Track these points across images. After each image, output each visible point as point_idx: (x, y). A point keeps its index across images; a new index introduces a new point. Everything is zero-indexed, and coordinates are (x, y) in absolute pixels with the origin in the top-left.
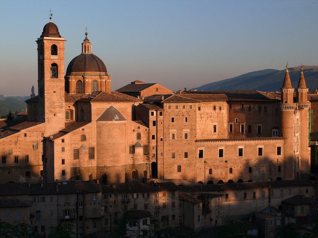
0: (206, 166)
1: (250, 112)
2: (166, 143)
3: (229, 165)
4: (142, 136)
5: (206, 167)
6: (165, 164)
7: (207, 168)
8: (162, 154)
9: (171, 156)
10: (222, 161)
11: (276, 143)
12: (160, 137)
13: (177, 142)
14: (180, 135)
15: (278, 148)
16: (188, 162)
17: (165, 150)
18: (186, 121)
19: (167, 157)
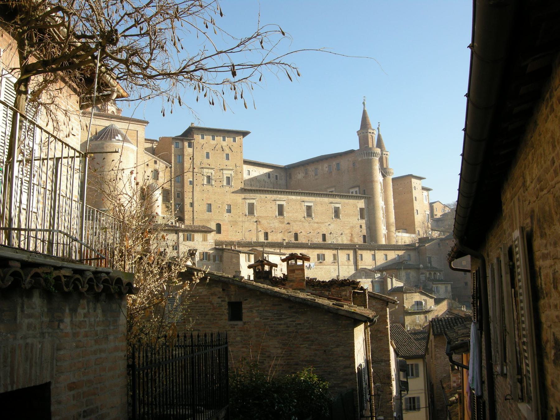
0: (259, 226)
1: (316, 177)
2: (197, 189)
3: (295, 228)
4: (161, 175)
5: (259, 229)
6: (195, 219)
8: (192, 205)
9: (205, 208)
10: (282, 223)
12: (189, 178)
13: (216, 189)
15: (360, 209)
17: (195, 199)
18: (228, 158)
19: (200, 207)
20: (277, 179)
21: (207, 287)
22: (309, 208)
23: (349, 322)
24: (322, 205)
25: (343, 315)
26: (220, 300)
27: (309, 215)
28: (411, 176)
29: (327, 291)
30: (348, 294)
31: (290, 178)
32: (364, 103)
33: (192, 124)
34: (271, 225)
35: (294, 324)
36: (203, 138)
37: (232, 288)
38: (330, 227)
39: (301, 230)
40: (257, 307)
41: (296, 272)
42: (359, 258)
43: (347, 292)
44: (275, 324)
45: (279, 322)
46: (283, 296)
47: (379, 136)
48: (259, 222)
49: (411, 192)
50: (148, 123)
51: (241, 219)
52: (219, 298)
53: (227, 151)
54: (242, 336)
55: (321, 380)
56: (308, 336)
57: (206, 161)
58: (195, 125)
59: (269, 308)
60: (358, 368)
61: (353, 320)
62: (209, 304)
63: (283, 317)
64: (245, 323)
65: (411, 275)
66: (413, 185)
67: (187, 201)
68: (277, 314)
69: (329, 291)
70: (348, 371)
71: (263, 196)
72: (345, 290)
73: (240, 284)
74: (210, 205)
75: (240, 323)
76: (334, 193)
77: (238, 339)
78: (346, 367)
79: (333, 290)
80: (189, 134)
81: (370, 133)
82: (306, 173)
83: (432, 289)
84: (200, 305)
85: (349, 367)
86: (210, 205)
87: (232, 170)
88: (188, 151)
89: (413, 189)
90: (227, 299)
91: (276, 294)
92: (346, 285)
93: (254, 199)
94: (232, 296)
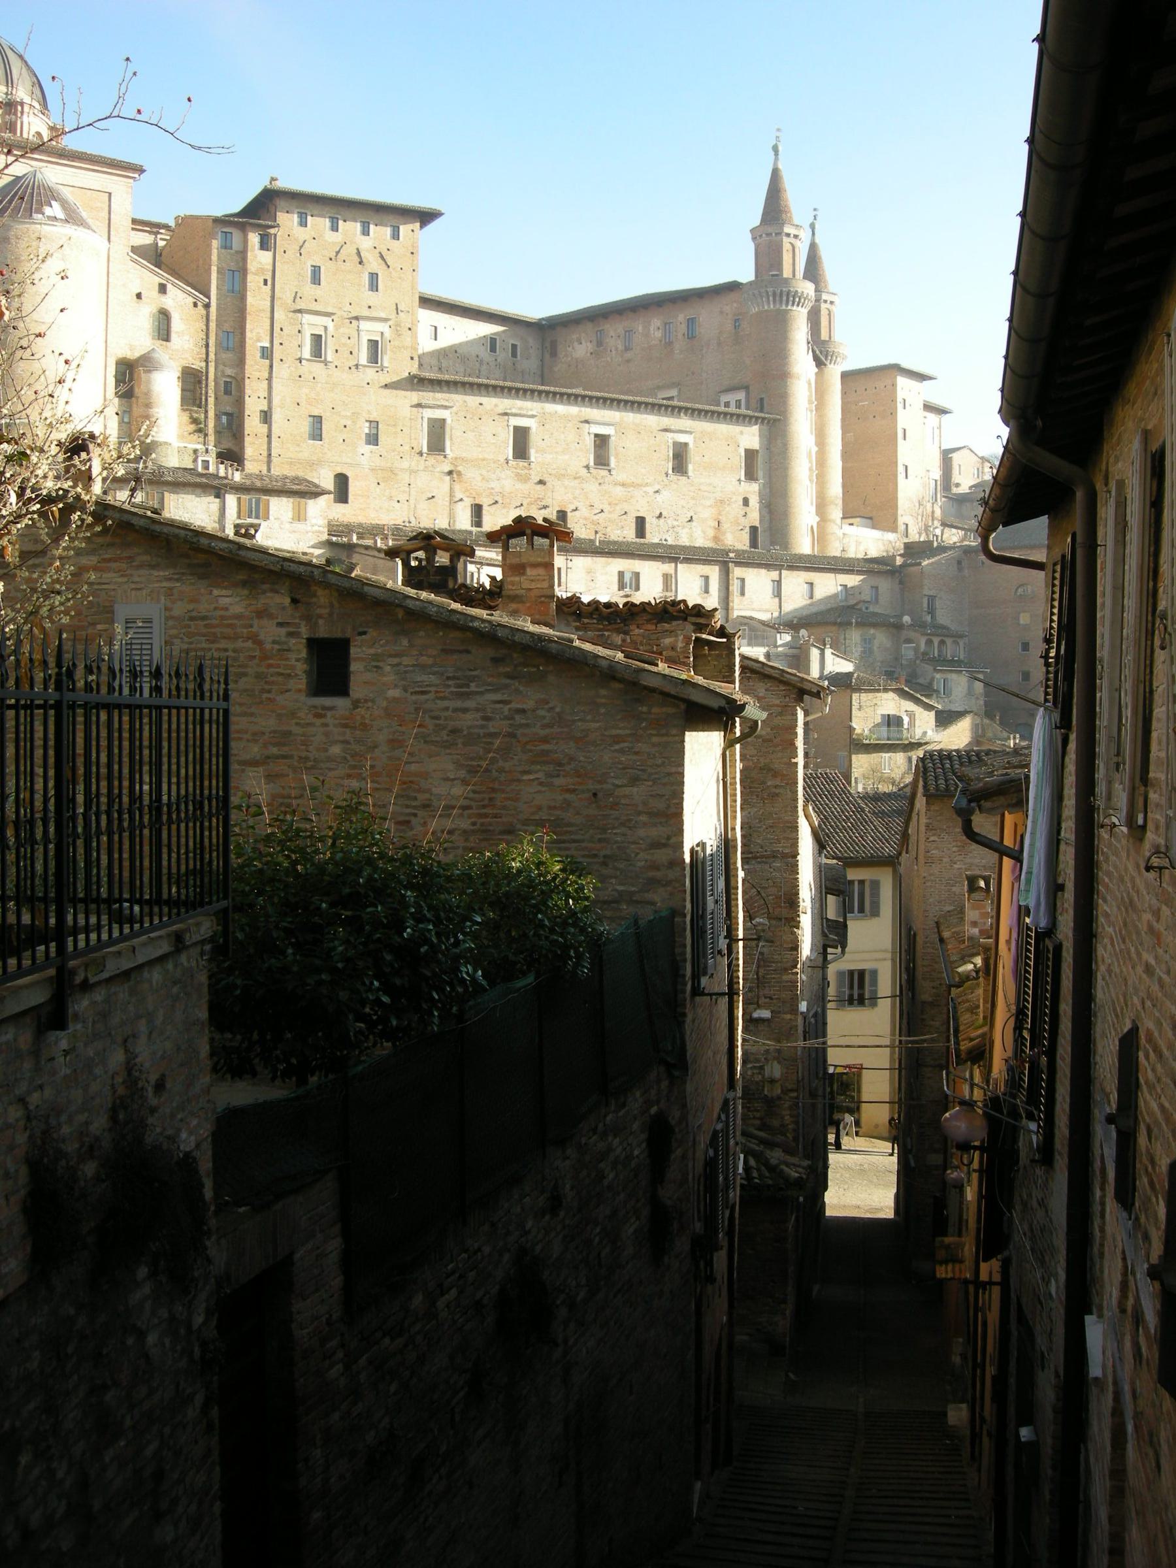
0: (457, 487)
4: (177, 325)
5: (458, 496)
6: (274, 460)
7: (461, 500)
8: (266, 417)
9: (305, 427)
10: (525, 479)
11: (742, 433)
12: (259, 340)
13: (337, 373)
14: (344, 345)
15: (747, 451)
16: (378, 462)
17: (276, 401)
18: (374, 284)
19: (289, 425)
20: (514, 354)
21: (246, 592)
22: (602, 442)
23: (671, 710)
24: (640, 435)
25: (652, 690)
26: (283, 631)
27: (602, 460)
28: (897, 369)
29: (619, 631)
30: (680, 645)
31: (554, 354)
32: (775, 149)
33: (273, 179)
34: (492, 485)
35: (506, 708)
36: (303, 223)
37: (322, 597)
38: (659, 498)
39: (577, 504)
40: (396, 656)
41: (529, 571)
42: (735, 587)
43: (680, 637)
44: (447, 709)
45: (459, 704)
46: (476, 624)
47: (813, 247)
48: (459, 473)
49: (893, 414)
50: (140, 170)
51: (405, 464)
52: (280, 625)
53: (374, 265)
54: (348, 742)
55: (572, 872)
56: (546, 747)
57: (309, 290)
58: (283, 184)
59: (430, 661)
60: (692, 850)
61: (683, 706)
62: (249, 644)
63: (473, 687)
64: (356, 704)
65: (876, 643)
66: (900, 395)
67: (253, 405)
68: (454, 678)
69: (626, 633)
70: (662, 856)
71: (472, 400)
72: (671, 632)
73: (347, 584)
74: (318, 420)
75: (340, 702)
76: (675, 403)
77: (336, 750)
78: (656, 845)
79: (637, 631)
80: (263, 208)
81: (788, 235)
82: (600, 343)
83: (931, 684)
84: (223, 644)
85: (665, 845)
86: (317, 421)
87: (386, 320)
88: (258, 259)
89: (900, 406)
90: (304, 631)
91: (454, 618)
92: (676, 618)
93: (446, 407)
94: (321, 622)
